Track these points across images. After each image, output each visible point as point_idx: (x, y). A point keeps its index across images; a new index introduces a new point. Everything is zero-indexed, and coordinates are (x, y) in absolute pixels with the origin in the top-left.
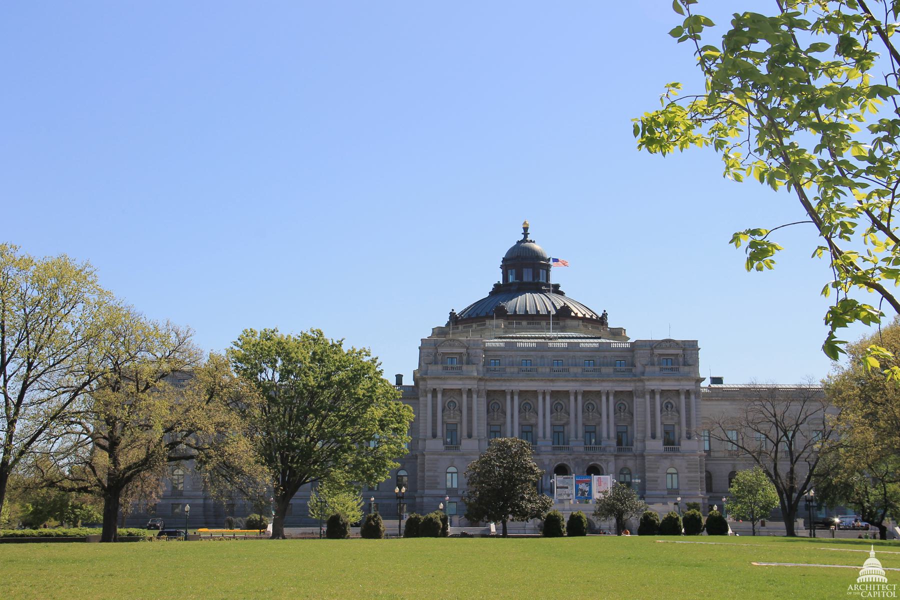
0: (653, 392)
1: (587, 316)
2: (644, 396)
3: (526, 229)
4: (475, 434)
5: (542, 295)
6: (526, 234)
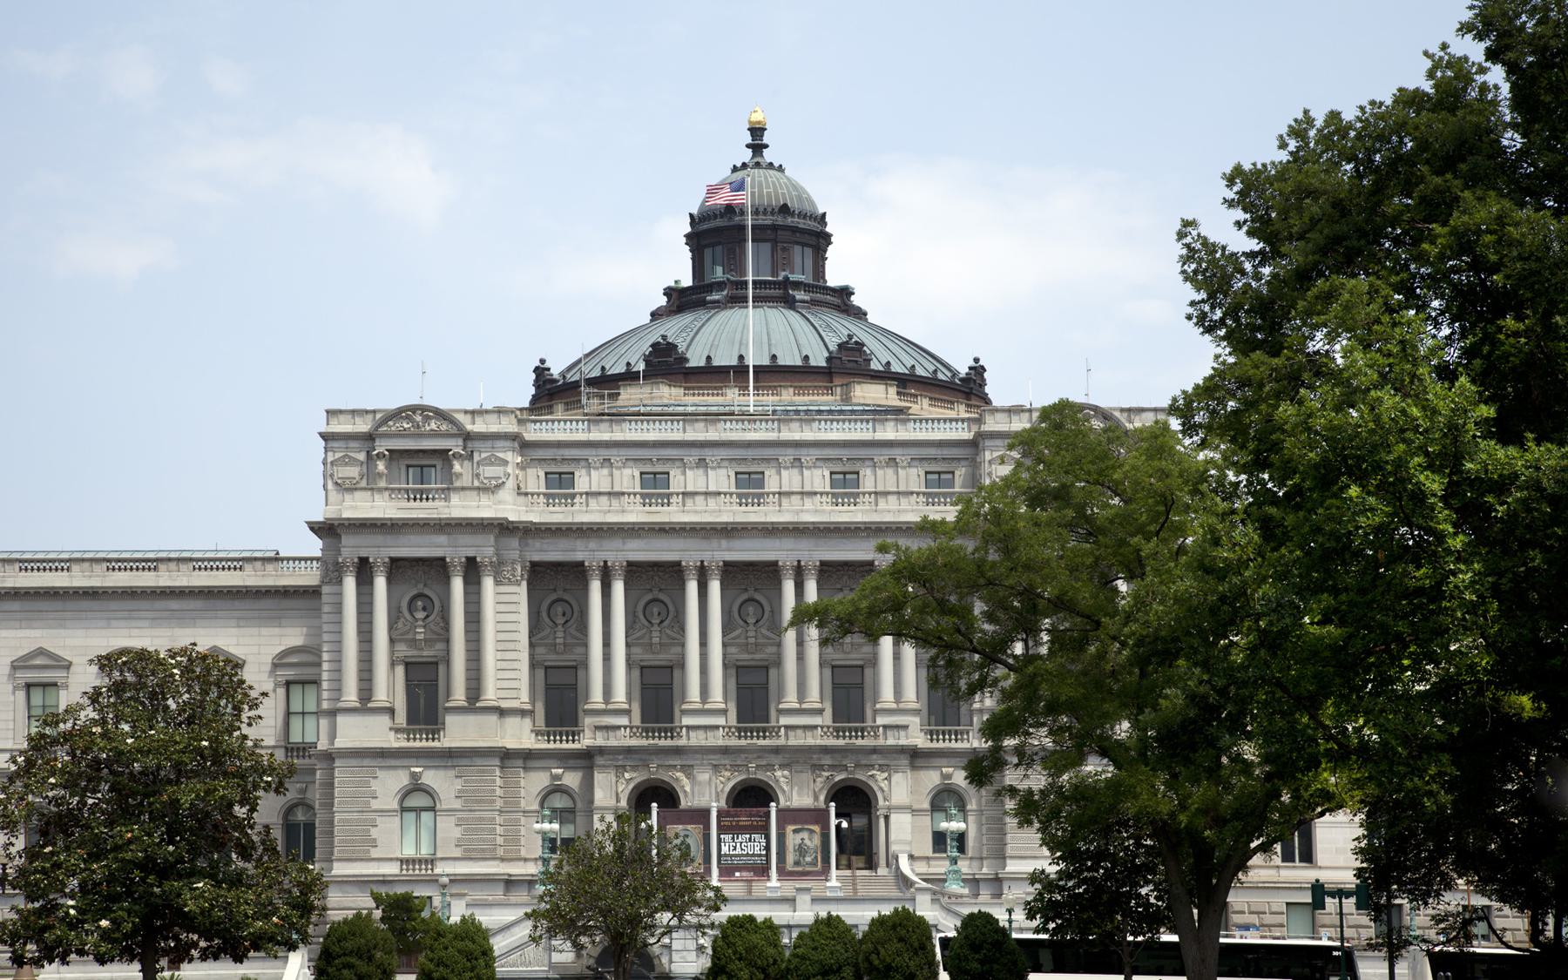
1: (920, 371)
3: (757, 131)
5: (791, 314)
6: (757, 148)
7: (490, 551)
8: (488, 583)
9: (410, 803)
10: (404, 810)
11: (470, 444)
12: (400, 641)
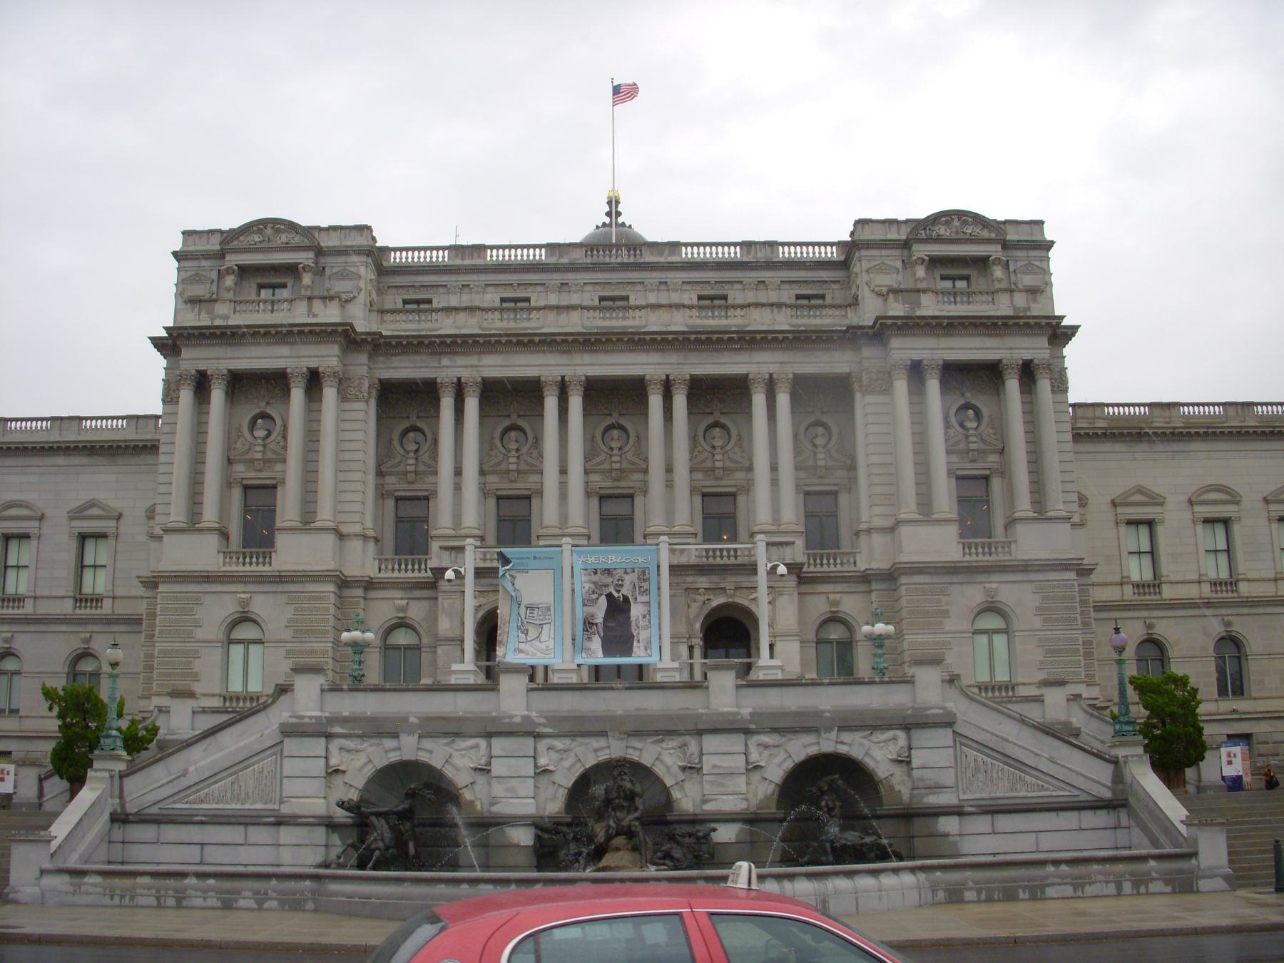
0: (916, 371)
2: (887, 389)
4: (325, 514)
7: (334, 362)
8: (330, 394)
10: (232, 642)
11: (322, 260)
12: (239, 461)
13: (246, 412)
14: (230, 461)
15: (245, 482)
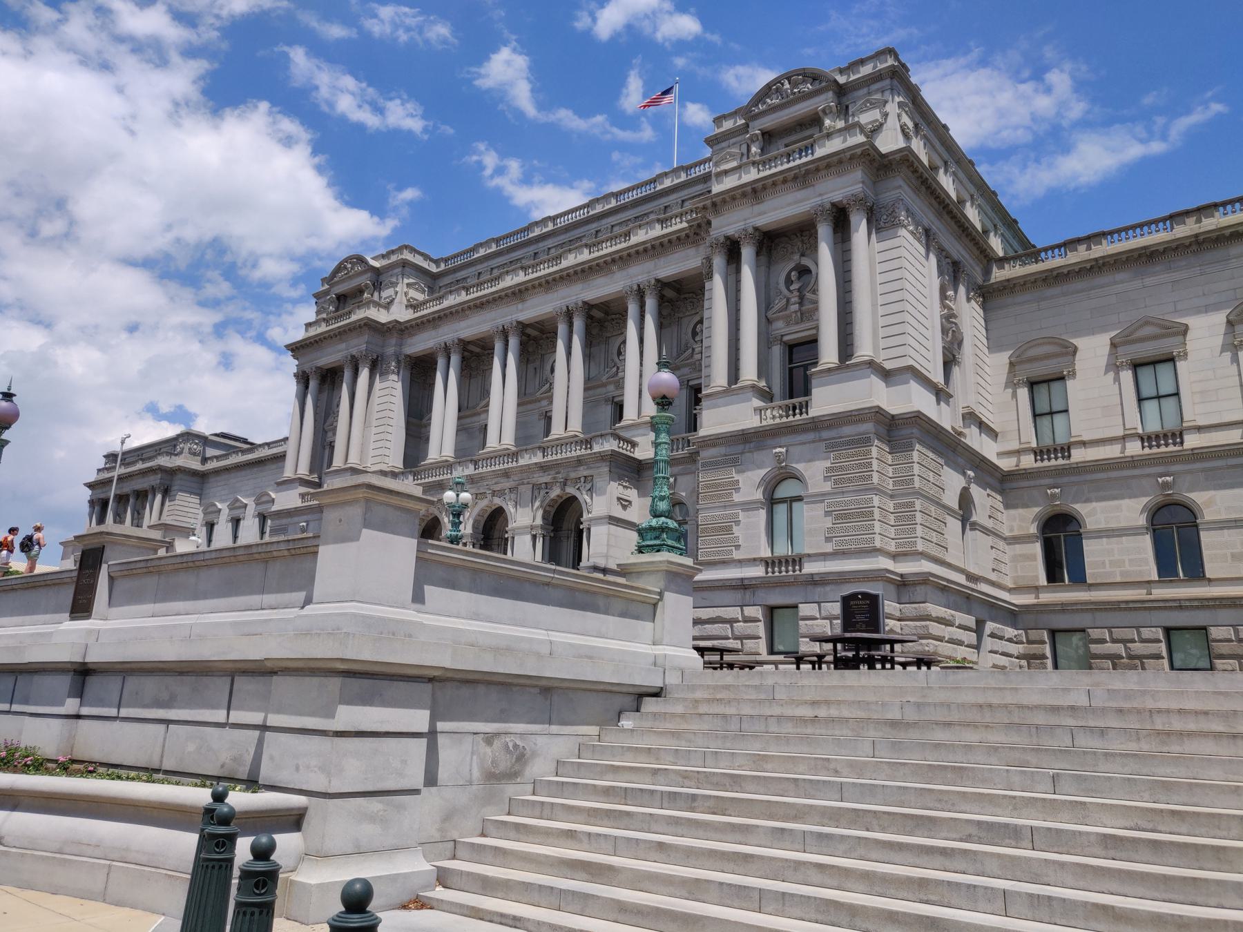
9: (782, 492)
12: (778, 319)
13: (784, 269)
14: (769, 321)
15: (785, 338)
